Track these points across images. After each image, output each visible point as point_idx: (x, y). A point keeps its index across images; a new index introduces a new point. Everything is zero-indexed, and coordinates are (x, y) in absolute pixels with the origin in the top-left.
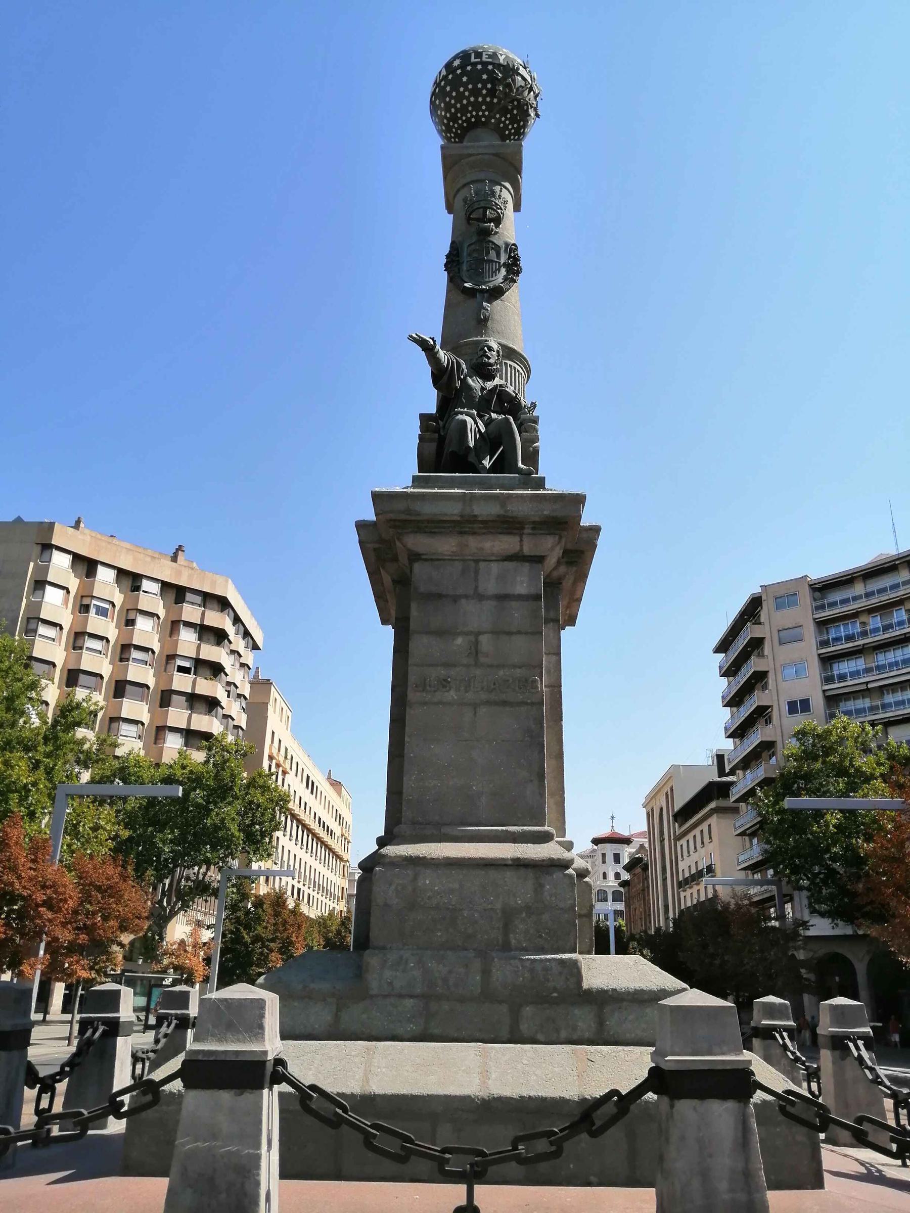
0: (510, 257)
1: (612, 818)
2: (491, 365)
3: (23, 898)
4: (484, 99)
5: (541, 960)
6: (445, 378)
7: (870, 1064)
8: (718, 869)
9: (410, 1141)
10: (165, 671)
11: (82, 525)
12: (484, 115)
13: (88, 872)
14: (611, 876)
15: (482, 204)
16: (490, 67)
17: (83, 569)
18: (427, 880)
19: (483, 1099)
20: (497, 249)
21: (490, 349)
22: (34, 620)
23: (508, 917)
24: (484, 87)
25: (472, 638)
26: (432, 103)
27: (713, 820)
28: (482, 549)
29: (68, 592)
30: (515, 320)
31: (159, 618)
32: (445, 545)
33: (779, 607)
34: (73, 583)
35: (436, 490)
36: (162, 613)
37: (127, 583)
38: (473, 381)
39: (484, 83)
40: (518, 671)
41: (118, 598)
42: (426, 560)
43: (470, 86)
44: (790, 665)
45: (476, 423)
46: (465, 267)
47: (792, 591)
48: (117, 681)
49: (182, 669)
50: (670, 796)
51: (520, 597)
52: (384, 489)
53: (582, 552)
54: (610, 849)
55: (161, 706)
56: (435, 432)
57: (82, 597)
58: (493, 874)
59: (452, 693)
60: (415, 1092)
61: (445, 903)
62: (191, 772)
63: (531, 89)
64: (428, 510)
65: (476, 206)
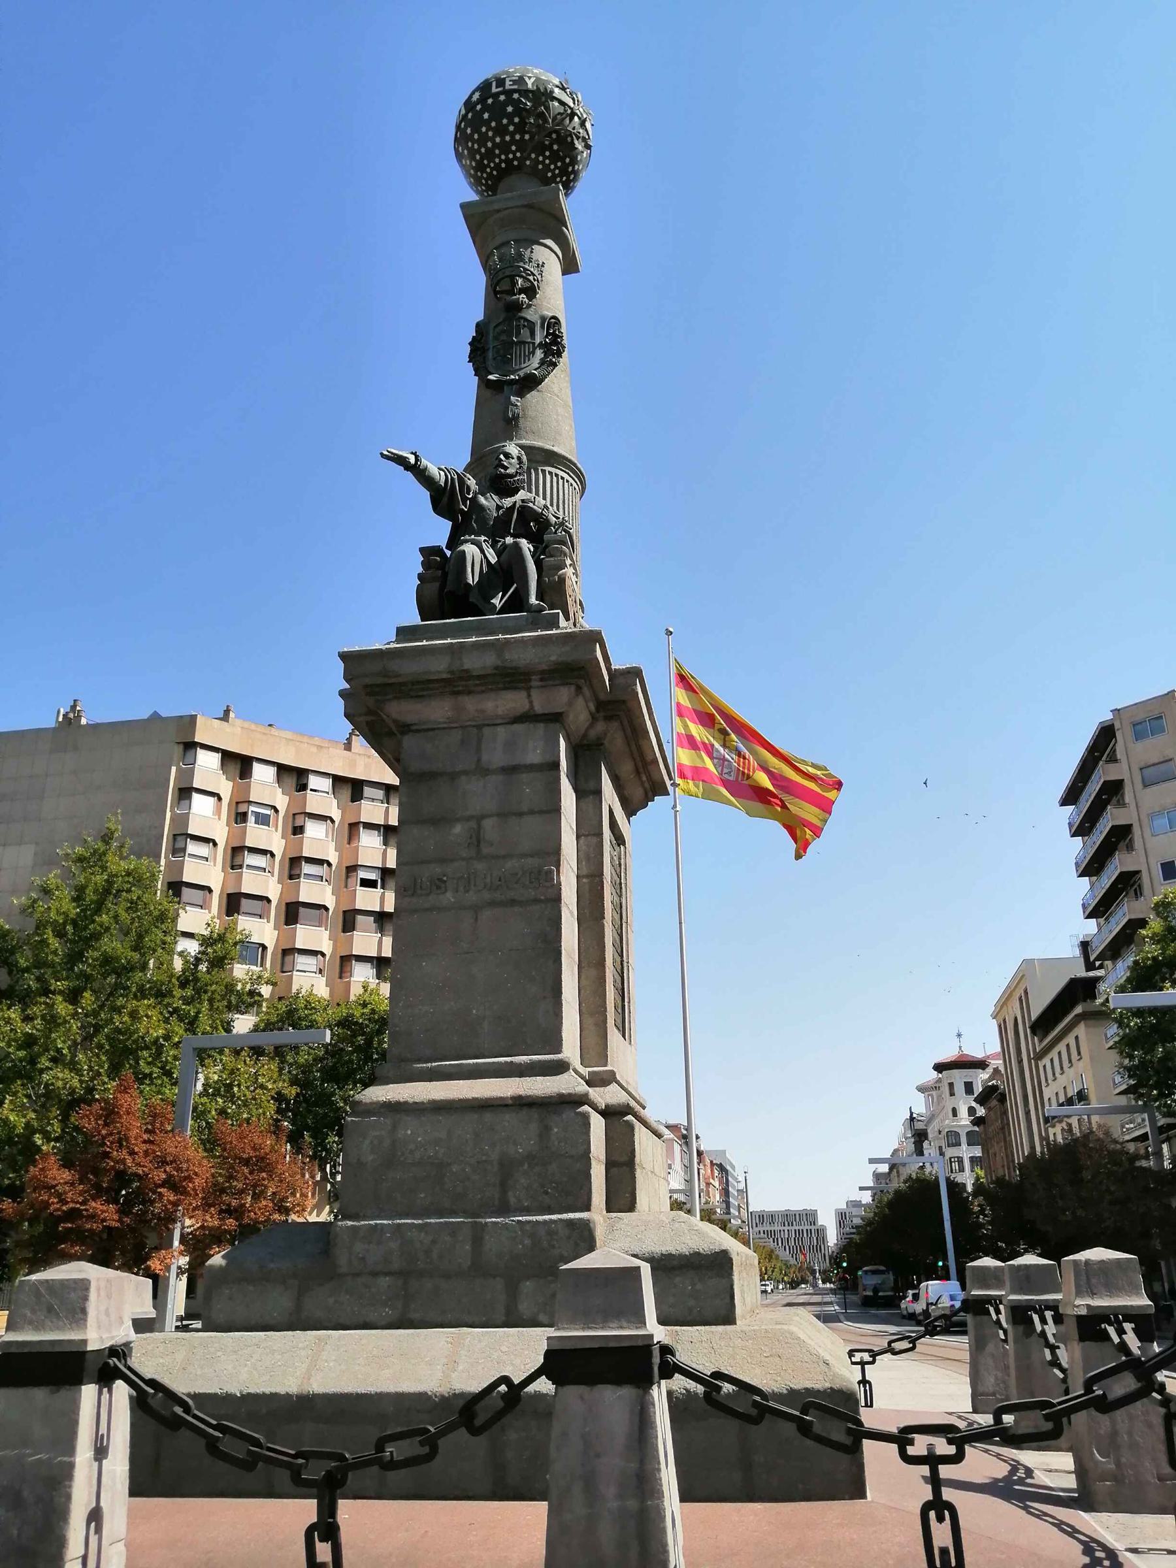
0: (548, 334)
1: (959, 1035)
2: (511, 476)
3: (140, 1178)
4: (512, 137)
5: (545, 1221)
6: (445, 500)
7: (1052, 1340)
8: (1093, 1097)
9: (257, 1443)
10: (346, 886)
11: (232, 715)
12: (515, 158)
13: (231, 1142)
14: (963, 1112)
15: (508, 273)
16: (516, 96)
17: (235, 768)
18: (409, 1129)
19: (443, 1396)
20: (531, 326)
21: (507, 456)
22: (182, 837)
23: (507, 1168)
24: (511, 122)
25: (473, 824)
26: (456, 150)
27: (1081, 1030)
28: (483, 711)
29: (220, 799)
30: (556, 412)
31: (333, 821)
32: (437, 710)
33: (1139, 736)
34: (225, 787)
35: (425, 643)
36: (336, 814)
37: (291, 781)
38: (486, 499)
39: (510, 117)
40: (530, 860)
41: (281, 801)
42: (418, 731)
44: (1160, 813)
45: (482, 551)
46: (490, 354)
47: (1156, 714)
48: (287, 904)
49: (366, 883)
51: (531, 768)
52: (357, 648)
53: (624, 702)
54: (959, 1077)
55: (344, 931)
56: (438, 569)
57: (237, 803)
58: (488, 1117)
59: (449, 895)
60: (361, 1389)
61: (430, 1157)
62: (373, 1011)
63: (573, 114)
64: (409, 669)
65: (501, 276)
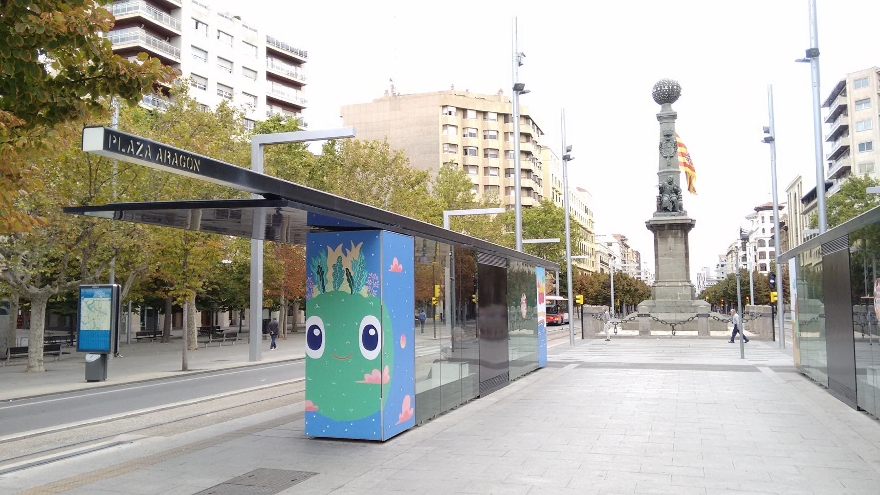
33: (857, 87)
50: (800, 186)
54: (767, 214)
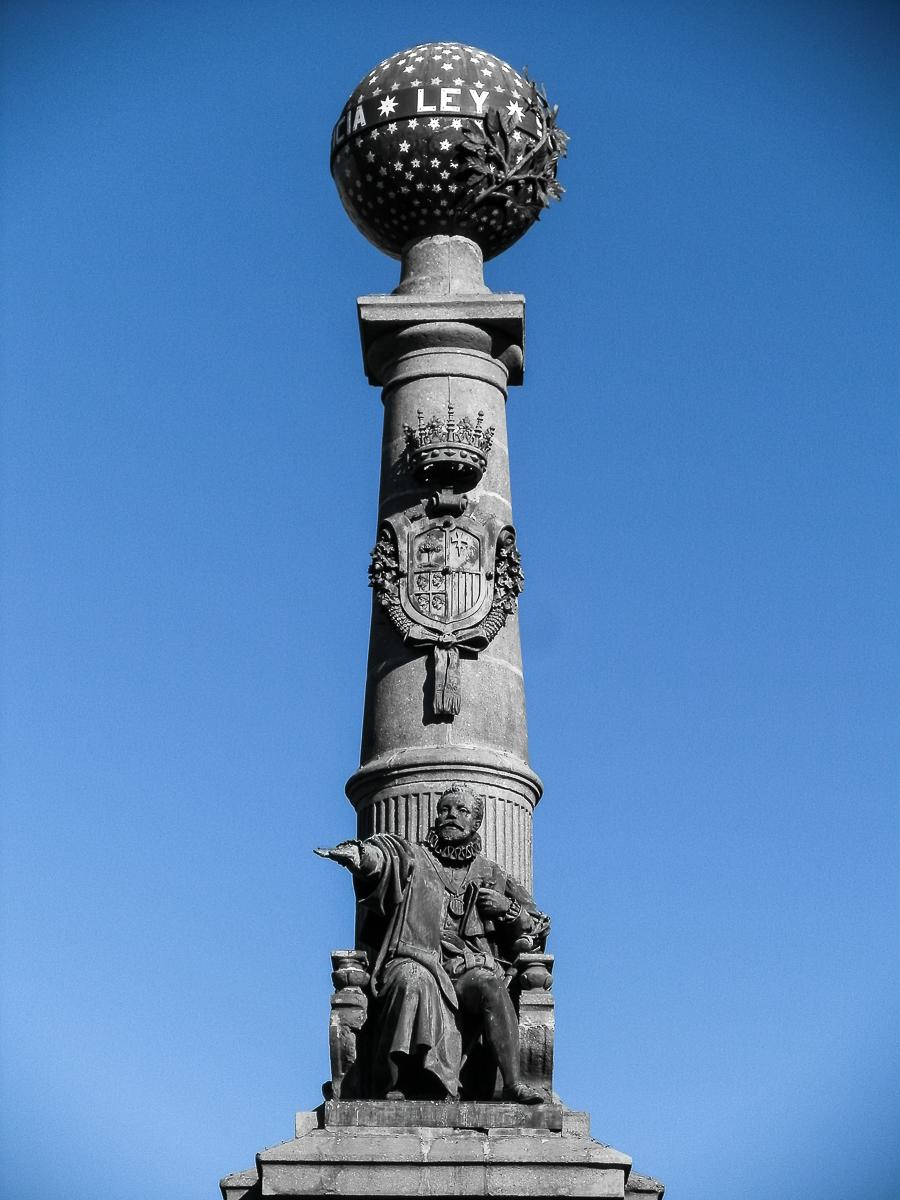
39: (444, 157)
43: (416, 163)
